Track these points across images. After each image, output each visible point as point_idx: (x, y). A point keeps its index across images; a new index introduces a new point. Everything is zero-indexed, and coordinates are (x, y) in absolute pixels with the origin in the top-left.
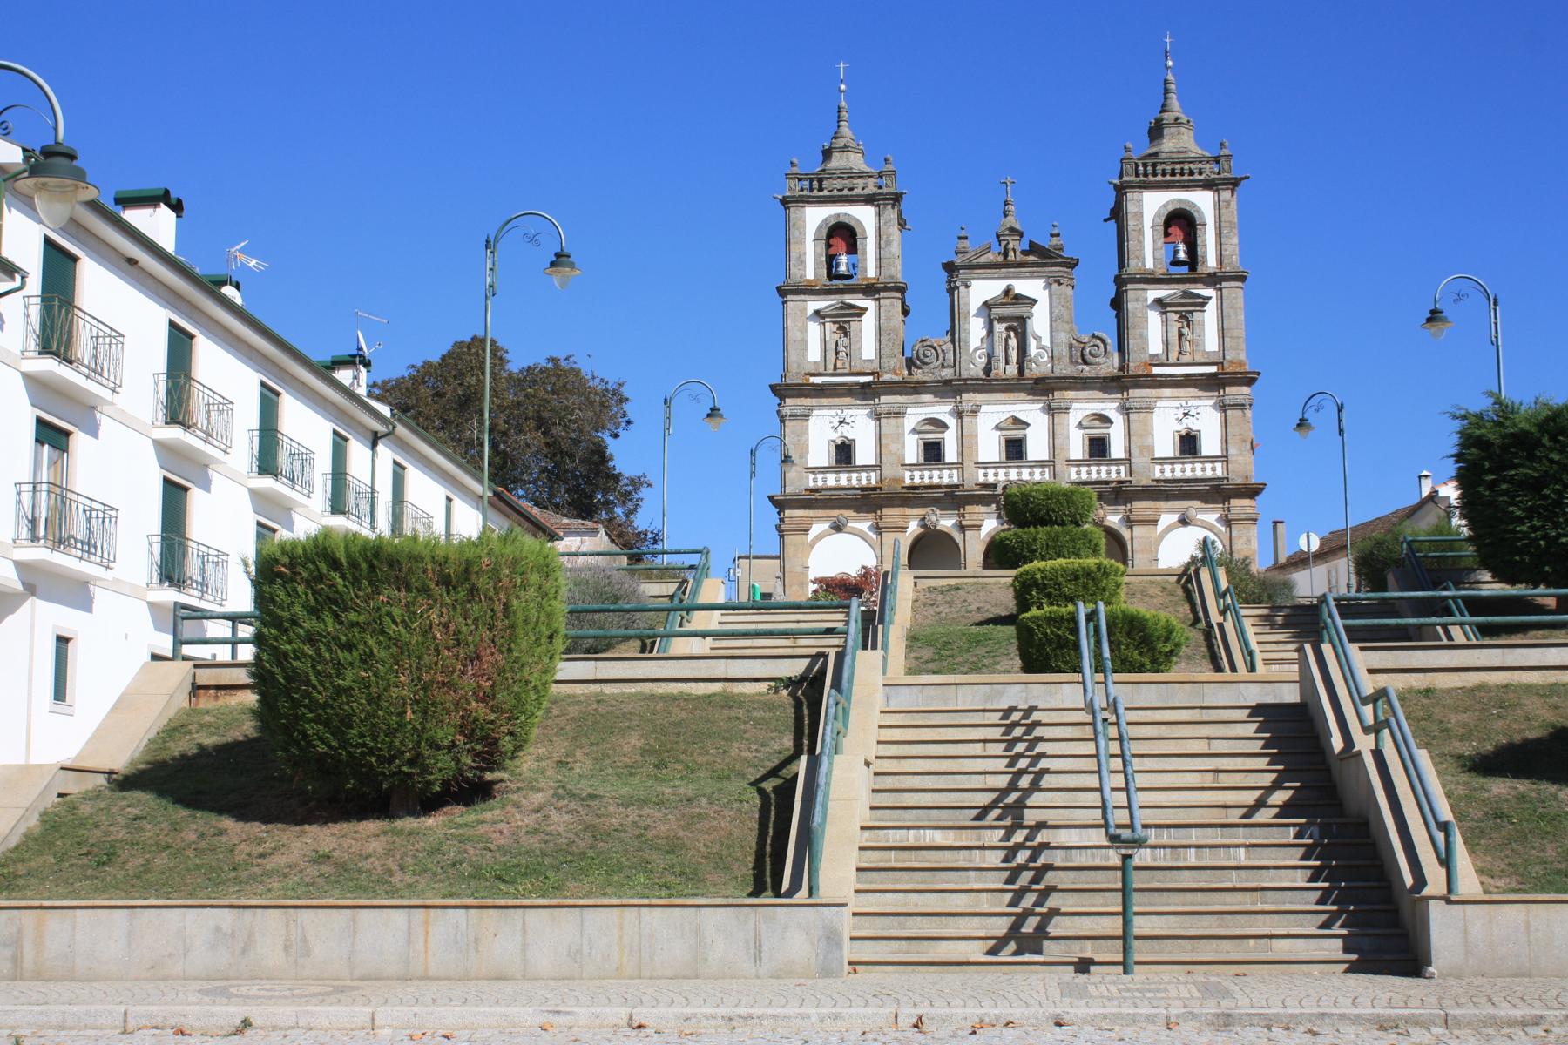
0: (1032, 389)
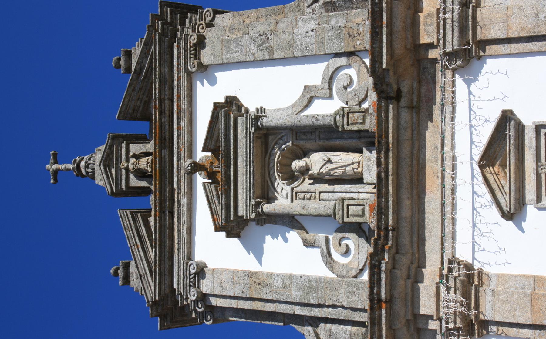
0: (411, 107)
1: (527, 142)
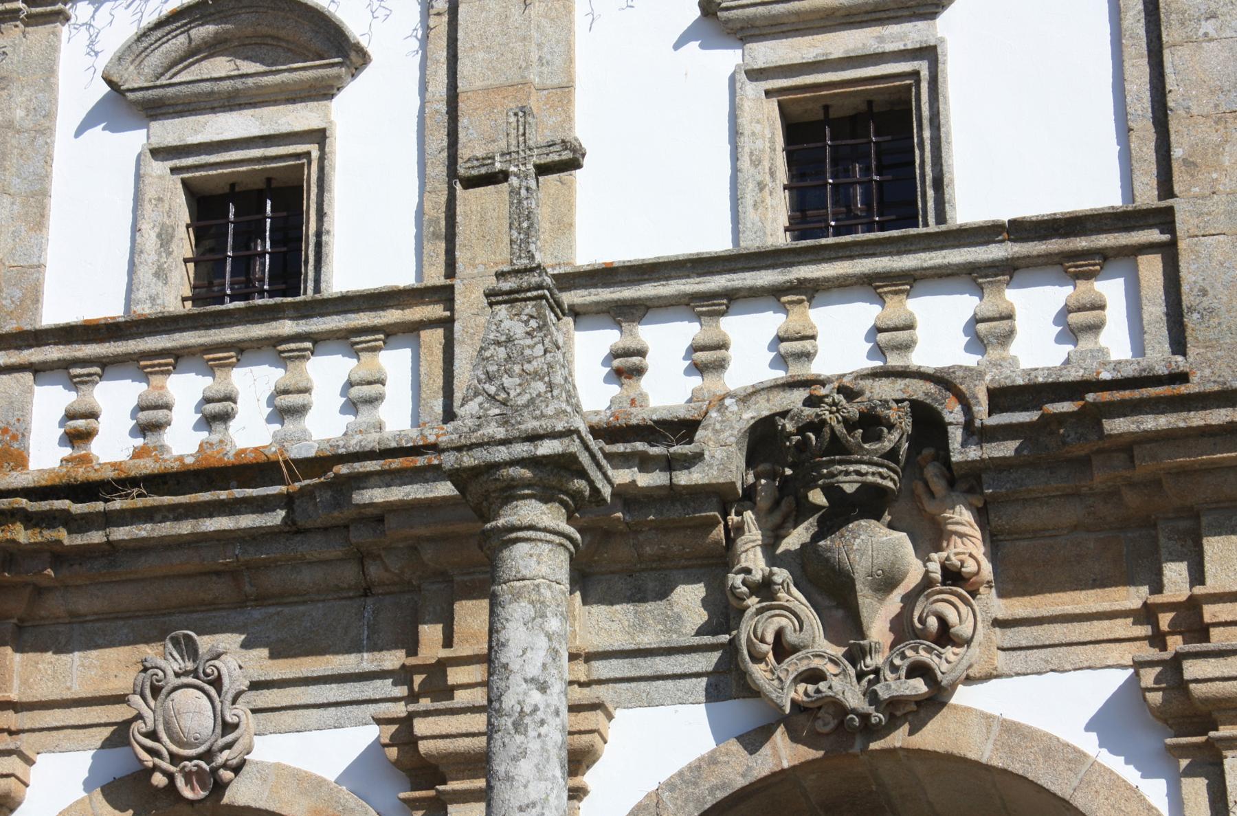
1: (894, 29)
